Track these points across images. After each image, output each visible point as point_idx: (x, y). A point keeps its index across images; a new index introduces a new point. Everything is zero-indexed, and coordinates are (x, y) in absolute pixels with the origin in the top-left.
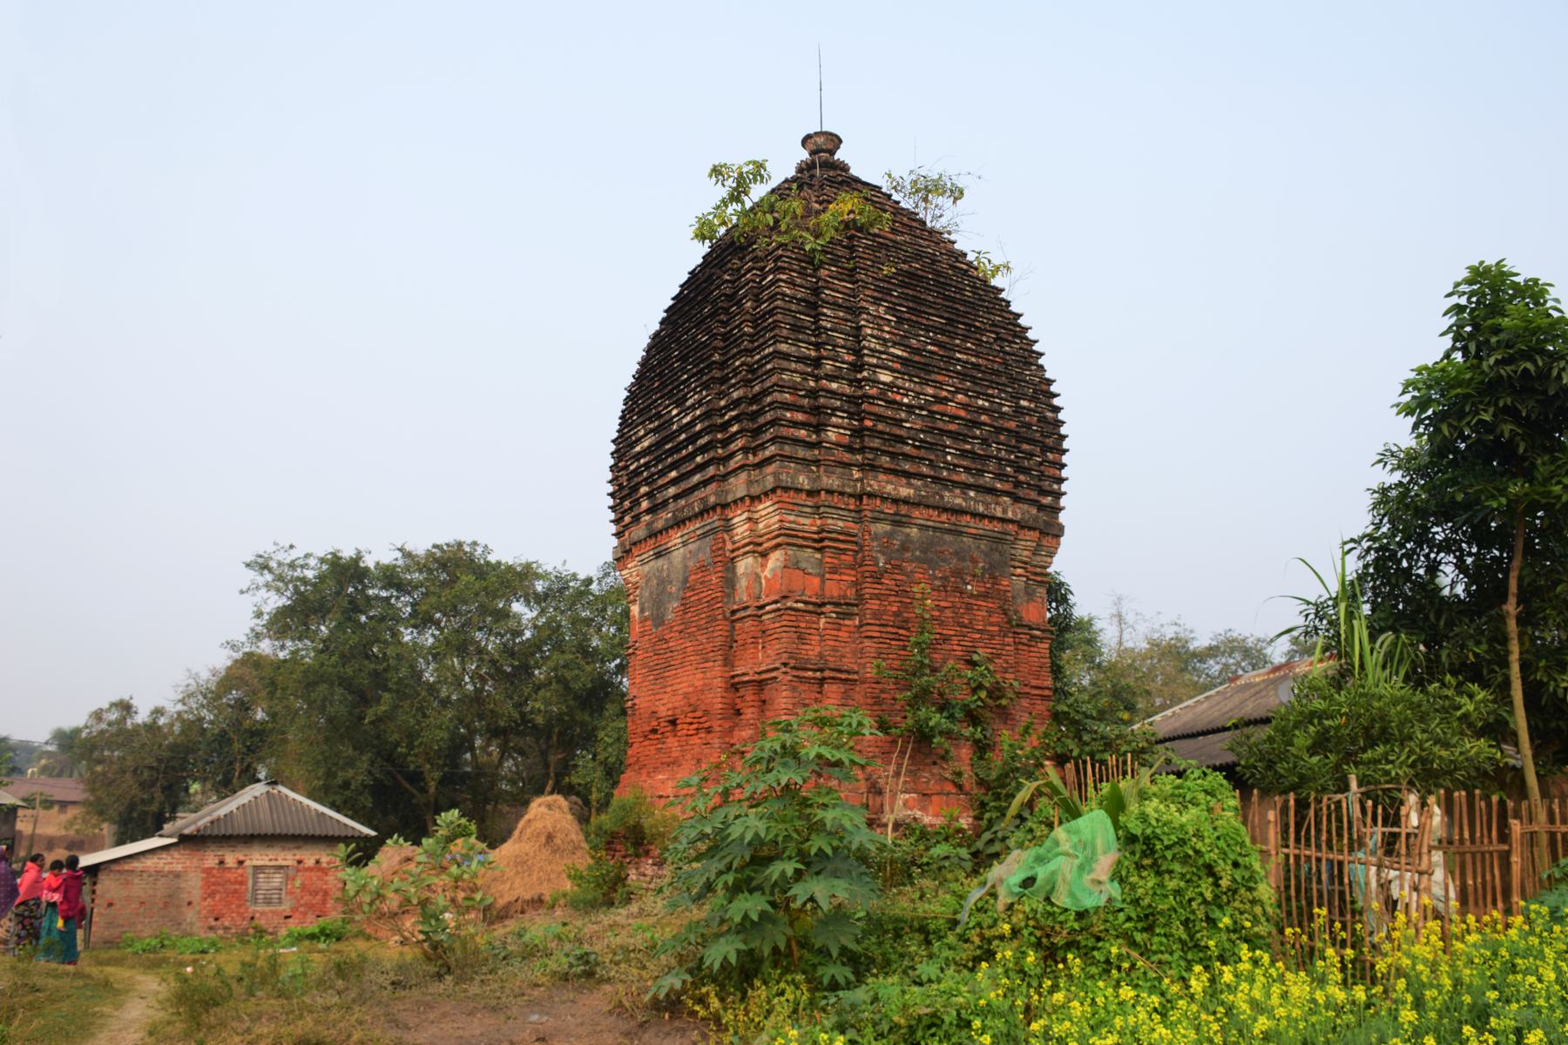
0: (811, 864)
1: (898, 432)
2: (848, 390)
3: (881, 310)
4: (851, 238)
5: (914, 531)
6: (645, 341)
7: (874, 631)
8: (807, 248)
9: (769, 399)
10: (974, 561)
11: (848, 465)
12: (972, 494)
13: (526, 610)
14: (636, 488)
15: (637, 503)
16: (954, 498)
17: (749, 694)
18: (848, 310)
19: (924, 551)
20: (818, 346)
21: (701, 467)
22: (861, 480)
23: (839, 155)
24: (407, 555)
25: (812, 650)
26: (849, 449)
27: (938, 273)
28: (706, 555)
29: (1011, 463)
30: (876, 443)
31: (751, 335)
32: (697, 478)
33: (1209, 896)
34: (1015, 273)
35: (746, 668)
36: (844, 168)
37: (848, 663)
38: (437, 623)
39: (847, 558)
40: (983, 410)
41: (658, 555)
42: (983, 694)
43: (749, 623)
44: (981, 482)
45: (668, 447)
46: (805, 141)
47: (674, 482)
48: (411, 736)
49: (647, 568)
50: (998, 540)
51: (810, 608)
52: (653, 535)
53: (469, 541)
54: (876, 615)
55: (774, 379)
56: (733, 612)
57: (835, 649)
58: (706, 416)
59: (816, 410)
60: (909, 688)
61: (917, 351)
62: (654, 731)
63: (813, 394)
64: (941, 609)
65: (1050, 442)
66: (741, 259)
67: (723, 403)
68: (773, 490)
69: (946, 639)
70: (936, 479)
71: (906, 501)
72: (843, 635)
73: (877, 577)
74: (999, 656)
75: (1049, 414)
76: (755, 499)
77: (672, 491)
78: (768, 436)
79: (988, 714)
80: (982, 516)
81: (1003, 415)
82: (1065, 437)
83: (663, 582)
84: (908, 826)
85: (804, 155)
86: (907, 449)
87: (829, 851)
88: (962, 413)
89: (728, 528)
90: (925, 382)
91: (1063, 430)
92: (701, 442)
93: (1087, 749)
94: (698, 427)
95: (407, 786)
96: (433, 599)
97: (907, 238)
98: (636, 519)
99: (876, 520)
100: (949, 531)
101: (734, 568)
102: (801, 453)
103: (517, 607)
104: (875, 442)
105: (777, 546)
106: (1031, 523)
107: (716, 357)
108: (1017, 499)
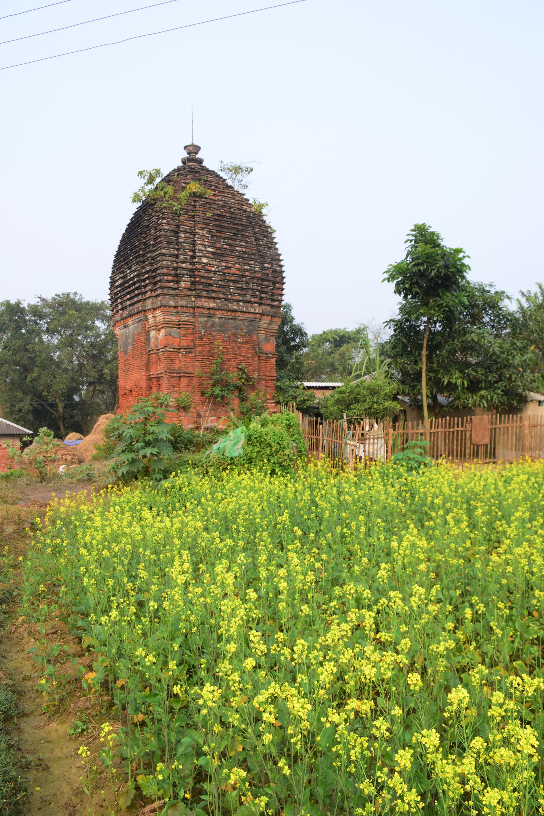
0: (148, 444)
1: (210, 282)
2: (190, 267)
3: (205, 232)
4: (195, 201)
5: (217, 320)
6: (120, 238)
7: (199, 358)
8: (174, 209)
9: (158, 272)
10: (242, 330)
11: (190, 296)
12: (241, 304)
13: (102, 325)
14: (116, 300)
15: (117, 306)
16: (233, 306)
17: (154, 381)
18: (191, 233)
19: (221, 327)
20: (178, 250)
21: (137, 295)
22: (194, 301)
23: (199, 156)
24: (43, 300)
25: (176, 366)
26: (190, 289)
27: (232, 213)
28: (140, 329)
29: (258, 290)
30: (201, 287)
31: (153, 245)
32: (136, 299)
33: (268, 453)
34: (270, 207)
35: (153, 373)
36: (200, 161)
37: (190, 370)
38: (59, 332)
39: (190, 331)
40: (247, 270)
41: (125, 327)
42: (243, 380)
43: (154, 356)
44: (245, 299)
45: (126, 285)
46: (185, 148)
47: (129, 299)
48: (49, 387)
49: (121, 331)
50: (252, 321)
51: (176, 350)
52: (123, 319)
53: (73, 292)
54: (200, 352)
55: (159, 264)
56: (149, 351)
57: (185, 365)
58: (138, 275)
59: (176, 275)
60: (212, 379)
61: (219, 249)
62: (125, 394)
63: (175, 269)
64: (228, 349)
65: (278, 280)
66: (152, 209)
67: (144, 271)
68: (160, 307)
69: (229, 360)
70: (226, 299)
71: (213, 309)
72: (188, 360)
73: (201, 338)
74: (251, 365)
75: (278, 268)
76: (154, 309)
77: (128, 303)
78: (158, 286)
79: (245, 387)
80: (245, 312)
81: (255, 272)
82: (284, 278)
83: (127, 338)
84: (212, 429)
85: (185, 155)
86: (214, 288)
87: (152, 440)
88: (238, 272)
89: (147, 320)
90: (222, 261)
91: (284, 275)
92: (137, 285)
93: (286, 400)
94: (136, 280)
95: (49, 409)
96: (55, 322)
97: (220, 198)
98: (117, 311)
99: (201, 316)
100: (231, 319)
101: (149, 335)
102: (171, 292)
103: (98, 323)
104: (201, 286)
105: (163, 327)
106: (267, 313)
107: (141, 252)
108: (260, 304)
